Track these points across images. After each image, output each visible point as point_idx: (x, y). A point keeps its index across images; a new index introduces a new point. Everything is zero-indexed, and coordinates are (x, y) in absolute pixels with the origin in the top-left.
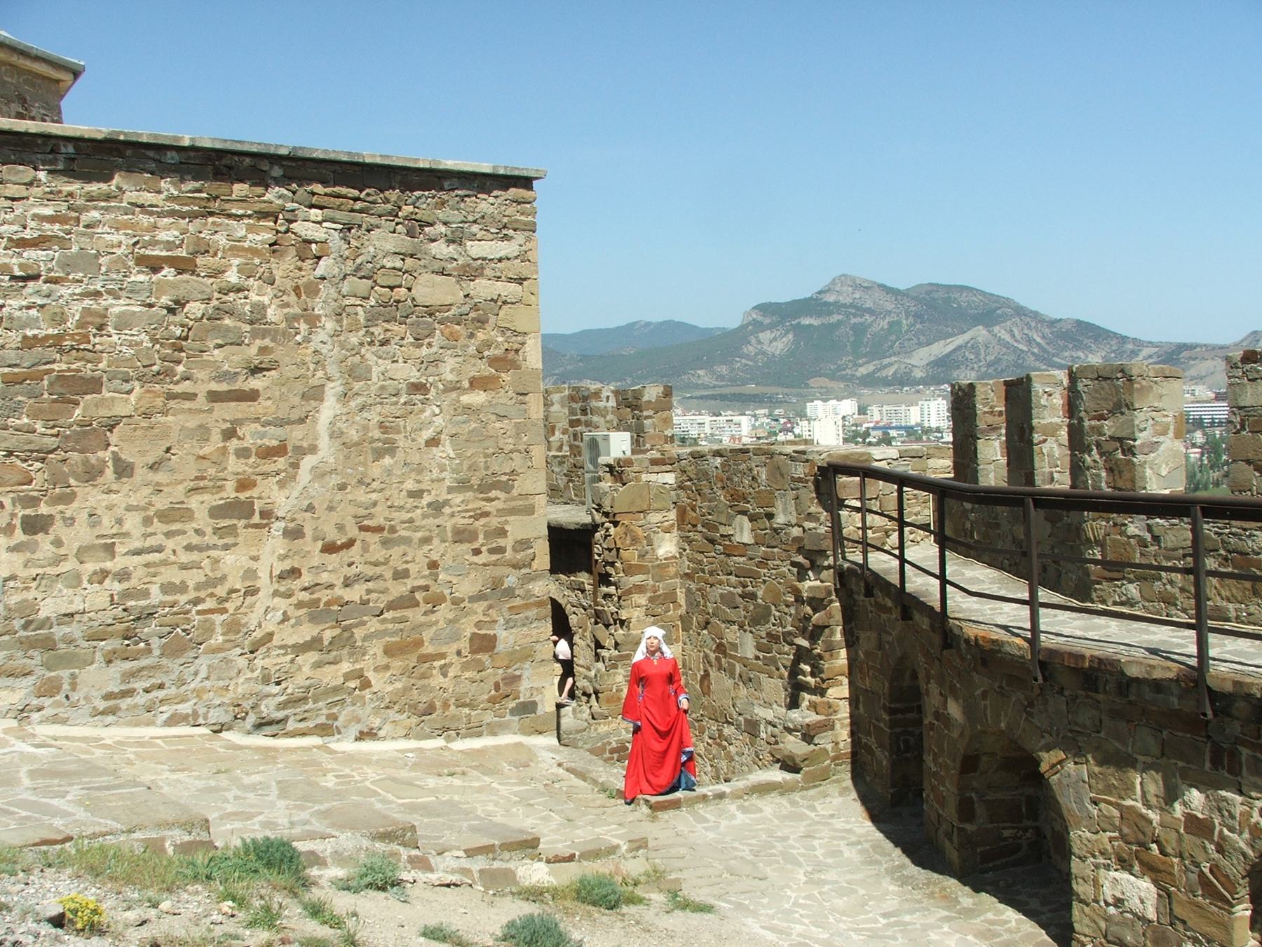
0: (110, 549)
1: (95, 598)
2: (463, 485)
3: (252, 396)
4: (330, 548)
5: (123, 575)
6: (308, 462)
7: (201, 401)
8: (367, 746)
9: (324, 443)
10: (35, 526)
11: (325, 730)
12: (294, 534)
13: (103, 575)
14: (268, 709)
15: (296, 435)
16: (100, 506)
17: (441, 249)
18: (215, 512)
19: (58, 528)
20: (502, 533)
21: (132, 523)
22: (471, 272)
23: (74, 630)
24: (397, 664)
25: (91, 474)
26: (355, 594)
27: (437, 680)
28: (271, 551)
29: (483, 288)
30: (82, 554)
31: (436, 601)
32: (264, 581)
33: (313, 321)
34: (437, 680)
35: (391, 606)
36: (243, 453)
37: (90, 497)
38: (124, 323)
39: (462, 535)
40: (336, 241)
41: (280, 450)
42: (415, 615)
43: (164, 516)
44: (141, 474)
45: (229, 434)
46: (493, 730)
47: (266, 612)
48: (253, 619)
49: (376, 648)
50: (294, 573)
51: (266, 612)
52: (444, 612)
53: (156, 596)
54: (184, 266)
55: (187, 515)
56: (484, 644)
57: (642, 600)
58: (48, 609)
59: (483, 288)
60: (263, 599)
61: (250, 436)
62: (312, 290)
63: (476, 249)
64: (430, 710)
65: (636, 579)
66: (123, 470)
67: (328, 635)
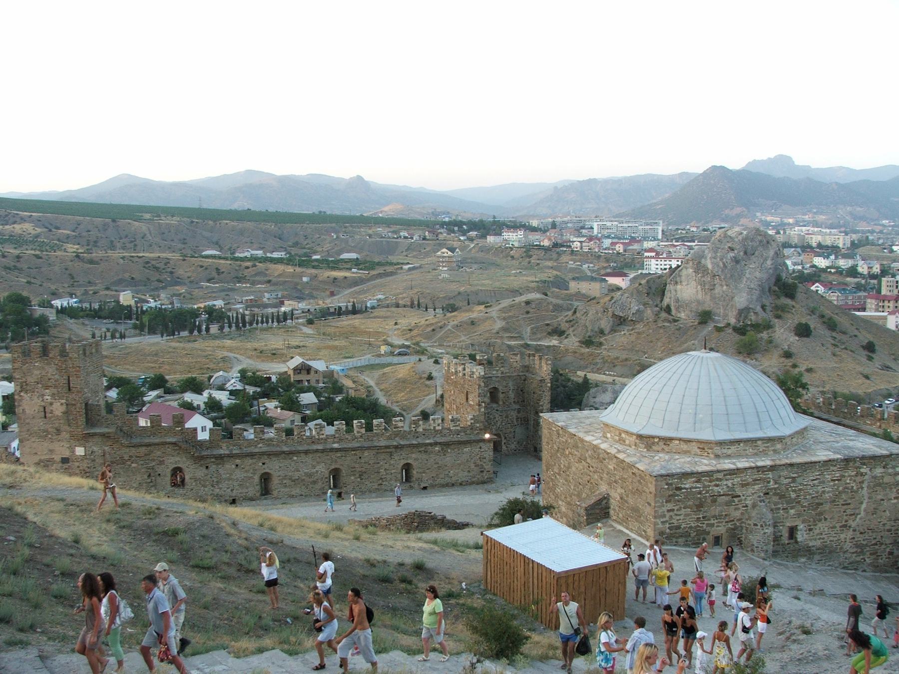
1: (818, 543)
2: (890, 520)
4: (861, 533)
6: (859, 516)
8: (864, 573)
9: (862, 513)
10: (810, 530)
11: (856, 569)
12: (854, 531)
15: (857, 511)
16: (822, 526)
17: (890, 471)
21: (826, 529)
24: (873, 557)
25: (820, 520)
27: (880, 561)
28: (850, 534)
30: (818, 534)
31: (882, 544)
32: (848, 540)
33: (862, 488)
34: (880, 561)
37: (820, 525)
38: (828, 492)
39: (889, 530)
40: (869, 472)
42: (877, 547)
46: (891, 572)
47: (848, 546)
49: (868, 553)
51: (848, 546)
52: (883, 546)
56: (891, 553)
58: (811, 544)
60: (847, 543)
61: (849, 512)
62: (862, 482)
66: (826, 519)
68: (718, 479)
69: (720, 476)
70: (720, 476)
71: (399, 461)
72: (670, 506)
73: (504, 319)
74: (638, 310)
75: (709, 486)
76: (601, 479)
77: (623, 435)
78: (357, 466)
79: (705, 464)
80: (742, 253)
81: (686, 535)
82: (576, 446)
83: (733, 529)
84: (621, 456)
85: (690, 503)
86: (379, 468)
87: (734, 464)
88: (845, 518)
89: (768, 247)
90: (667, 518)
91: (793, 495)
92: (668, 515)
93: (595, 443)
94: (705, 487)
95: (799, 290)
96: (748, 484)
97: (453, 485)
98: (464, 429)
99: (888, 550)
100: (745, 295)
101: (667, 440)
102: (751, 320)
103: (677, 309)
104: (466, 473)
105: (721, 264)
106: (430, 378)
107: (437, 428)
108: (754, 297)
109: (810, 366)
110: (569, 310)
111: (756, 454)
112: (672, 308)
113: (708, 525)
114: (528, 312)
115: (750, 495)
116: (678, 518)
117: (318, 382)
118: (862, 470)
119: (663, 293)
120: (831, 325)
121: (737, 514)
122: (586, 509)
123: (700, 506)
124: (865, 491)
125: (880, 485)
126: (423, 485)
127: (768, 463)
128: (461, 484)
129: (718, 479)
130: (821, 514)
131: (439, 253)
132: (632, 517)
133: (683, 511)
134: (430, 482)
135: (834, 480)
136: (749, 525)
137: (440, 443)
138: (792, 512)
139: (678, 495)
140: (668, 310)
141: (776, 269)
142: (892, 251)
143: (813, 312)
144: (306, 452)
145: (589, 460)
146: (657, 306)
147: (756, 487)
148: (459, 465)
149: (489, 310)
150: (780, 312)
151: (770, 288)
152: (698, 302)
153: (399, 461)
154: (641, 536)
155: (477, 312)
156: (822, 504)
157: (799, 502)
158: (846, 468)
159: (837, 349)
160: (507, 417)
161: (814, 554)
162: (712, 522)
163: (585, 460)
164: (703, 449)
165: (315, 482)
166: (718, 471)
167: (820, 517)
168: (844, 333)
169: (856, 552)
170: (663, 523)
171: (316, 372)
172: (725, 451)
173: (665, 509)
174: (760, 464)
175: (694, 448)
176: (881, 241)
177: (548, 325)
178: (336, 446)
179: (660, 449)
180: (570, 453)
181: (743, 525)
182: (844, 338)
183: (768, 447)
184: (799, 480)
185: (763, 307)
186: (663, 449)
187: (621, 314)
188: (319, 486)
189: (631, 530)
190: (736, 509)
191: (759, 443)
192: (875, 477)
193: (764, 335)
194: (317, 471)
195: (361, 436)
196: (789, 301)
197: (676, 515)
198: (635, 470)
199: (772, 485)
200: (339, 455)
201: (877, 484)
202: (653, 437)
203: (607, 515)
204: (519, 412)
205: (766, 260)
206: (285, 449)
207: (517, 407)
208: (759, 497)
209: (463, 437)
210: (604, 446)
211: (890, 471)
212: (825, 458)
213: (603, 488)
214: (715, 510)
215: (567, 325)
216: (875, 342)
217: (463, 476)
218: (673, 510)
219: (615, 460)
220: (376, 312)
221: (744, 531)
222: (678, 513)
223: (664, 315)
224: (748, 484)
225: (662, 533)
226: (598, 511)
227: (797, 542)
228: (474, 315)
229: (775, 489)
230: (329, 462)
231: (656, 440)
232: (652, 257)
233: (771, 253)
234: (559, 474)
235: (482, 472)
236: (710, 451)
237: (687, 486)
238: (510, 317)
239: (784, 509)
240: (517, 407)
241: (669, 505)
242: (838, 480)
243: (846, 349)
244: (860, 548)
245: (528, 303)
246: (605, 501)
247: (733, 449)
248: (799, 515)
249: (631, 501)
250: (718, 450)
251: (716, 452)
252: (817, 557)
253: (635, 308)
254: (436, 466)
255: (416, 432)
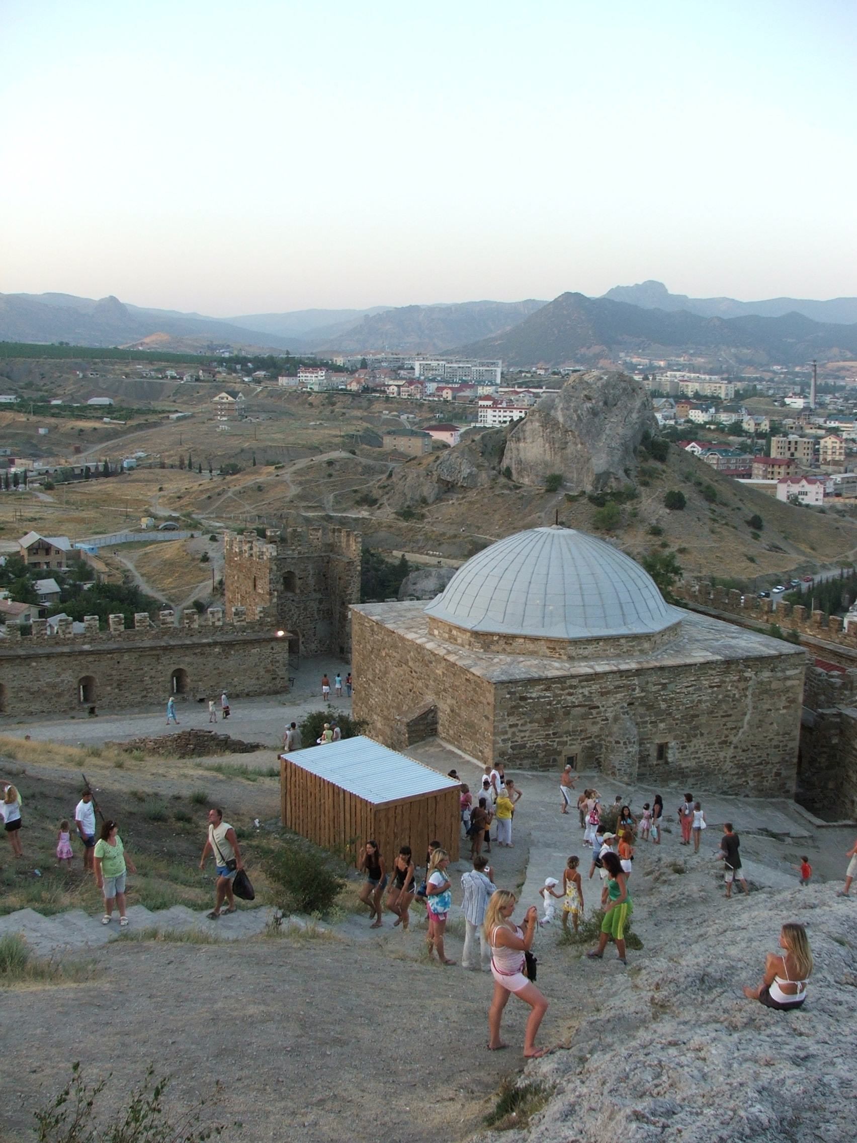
0: (697, 752)
1: (693, 764)
2: (778, 734)
3: (730, 716)
4: (744, 751)
5: (699, 758)
6: (741, 731)
7: (720, 718)
8: (746, 799)
9: (746, 726)
10: (684, 748)
11: (736, 794)
12: (736, 747)
13: (695, 758)
14: (725, 789)
15: (740, 724)
16: (697, 743)
17: (779, 674)
18: (719, 743)
19: (688, 748)
20: (786, 746)
21: (702, 747)
22: (787, 678)
23: (688, 770)
24: (757, 779)
25: (695, 736)
26: (747, 762)
28: (730, 752)
29: (789, 683)
30: (692, 753)
32: (728, 760)
33: (746, 696)
35: (758, 764)
36: (727, 729)
37: (695, 741)
38: (706, 701)
39: (776, 747)
40: (754, 677)
41: (735, 728)
42: (761, 767)
43: (709, 745)
44: (705, 735)
45: (725, 725)
46: (777, 797)
48: (724, 768)
49: (751, 775)
50: (735, 757)
52: (770, 766)
53: (705, 762)
54: (718, 686)
55: (713, 744)
56: (778, 774)
57: (825, 756)
58: (684, 765)
59: (789, 683)
61: (729, 725)
62: (747, 689)
63: (788, 673)
64: (762, 790)
65: (825, 749)
67: (741, 771)
68: (571, 687)
69: (575, 682)
70: (575, 682)
71: (168, 666)
72: (513, 720)
73: (300, 483)
74: (470, 474)
75: (561, 695)
76: (427, 686)
77: (454, 632)
78: (114, 672)
79: (556, 668)
80: (601, 404)
81: (533, 755)
82: (394, 646)
83: (591, 748)
84: (452, 658)
85: (537, 716)
86: (143, 675)
87: (592, 667)
88: (726, 732)
89: (633, 396)
90: (509, 736)
91: (663, 706)
92: (510, 731)
93: (419, 641)
94: (556, 696)
95: (671, 450)
96: (608, 693)
97: (238, 696)
98: (251, 625)
99: (775, 770)
100: (604, 455)
101: (509, 639)
102: (611, 488)
103: (519, 473)
104: (254, 681)
105: (575, 417)
106: (205, 559)
107: (217, 624)
108: (616, 459)
109: (684, 545)
110: (382, 473)
111: (619, 655)
112: (514, 471)
113: (559, 743)
114: (330, 476)
115: (611, 706)
116: (523, 734)
117: (60, 564)
118: (746, 674)
119: (501, 453)
120: (710, 495)
121: (595, 729)
122: (408, 725)
123: (549, 720)
124: (749, 700)
125: (766, 692)
126: (199, 697)
127: (634, 666)
128: (247, 695)
129: (571, 687)
130: (696, 728)
131: (217, 399)
132: (465, 734)
133: (529, 727)
134: (208, 693)
135: (713, 687)
136: (611, 742)
137: (221, 643)
138: (662, 726)
139: (522, 707)
140: (508, 473)
141: (643, 424)
142: (784, 404)
143: (687, 478)
144: (49, 656)
145: (410, 664)
146: (494, 469)
147: (619, 696)
148: (245, 670)
149: (280, 472)
150: (647, 478)
151: (635, 448)
152: (546, 465)
153: (168, 666)
154: (478, 758)
155: (266, 474)
156: (698, 716)
157: (670, 714)
158: (726, 672)
159: (716, 525)
160: (305, 609)
161: (688, 776)
162: (565, 739)
163: (406, 663)
164: (554, 649)
165: (59, 695)
166: (573, 677)
167: (695, 732)
168: (725, 505)
169: (737, 774)
170: (504, 741)
171: (58, 551)
172: (581, 651)
173: (506, 724)
174: (623, 667)
175: (543, 648)
176: (771, 392)
177: (355, 491)
178: (86, 647)
179: (500, 649)
180: (387, 654)
181: (603, 742)
182: (725, 511)
183: (633, 646)
184: (670, 687)
185: (627, 472)
186: (504, 650)
187: (449, 479)
188: (65, 699)
189: (465, 751)
190: (594, 723)
191: (623, 641)
192: (761, 683)
193: (628, 506)
194: (63, 681)
195: (119, 635)
196: (658, 465)
197: (521, 731)
198: (469, 676)
199: (637, 693)
200: (90, 659)
201: (764, 691)
202: (492, 634)
203: (434, 732)
204: (320, 602)
205: (631, 412)
206: (21, 652)
207: (319, 596)
208: (622, 708)
209: (249, 635)
210: (430, 646)
211: (779, 674)
212: (702, 660)
213: (430, 698)
214: (569, 725)
215: (380, 492)
216: (762, 515)
217: (250, 684)
218: (517, 725)
219: (444, 664)
220: (136, 474)
221: (604, 750)
222: (524, 728)
223: (503, 480)
224: (608, 693)
225: (502, 754)
226: (422, 727)
227: (667, 763)
228: (261, 479)
229: (642, 698)
230: (78, 668)
231: (495, 638)
232: (487, 407)
233: (638, 403)
234: (373, 682)
235: (274, 679)
236: (562, 651)
237: (534, 695)
238: (307, 482)
239: (651, 722)
240: (319, 596)
241: (511, 718)
242: (718, 686)
243: (726, 524)
244: (743, 768)
245: (330, 463)
246: (431, 715)
247: (591, 649)
248: (670, 730)
249: (464, 714)
250: (572, 651)
251: (570, 652)
252: (691, 781)
253: (466, 471)
254: (215, 672)
255: (190, 629)
